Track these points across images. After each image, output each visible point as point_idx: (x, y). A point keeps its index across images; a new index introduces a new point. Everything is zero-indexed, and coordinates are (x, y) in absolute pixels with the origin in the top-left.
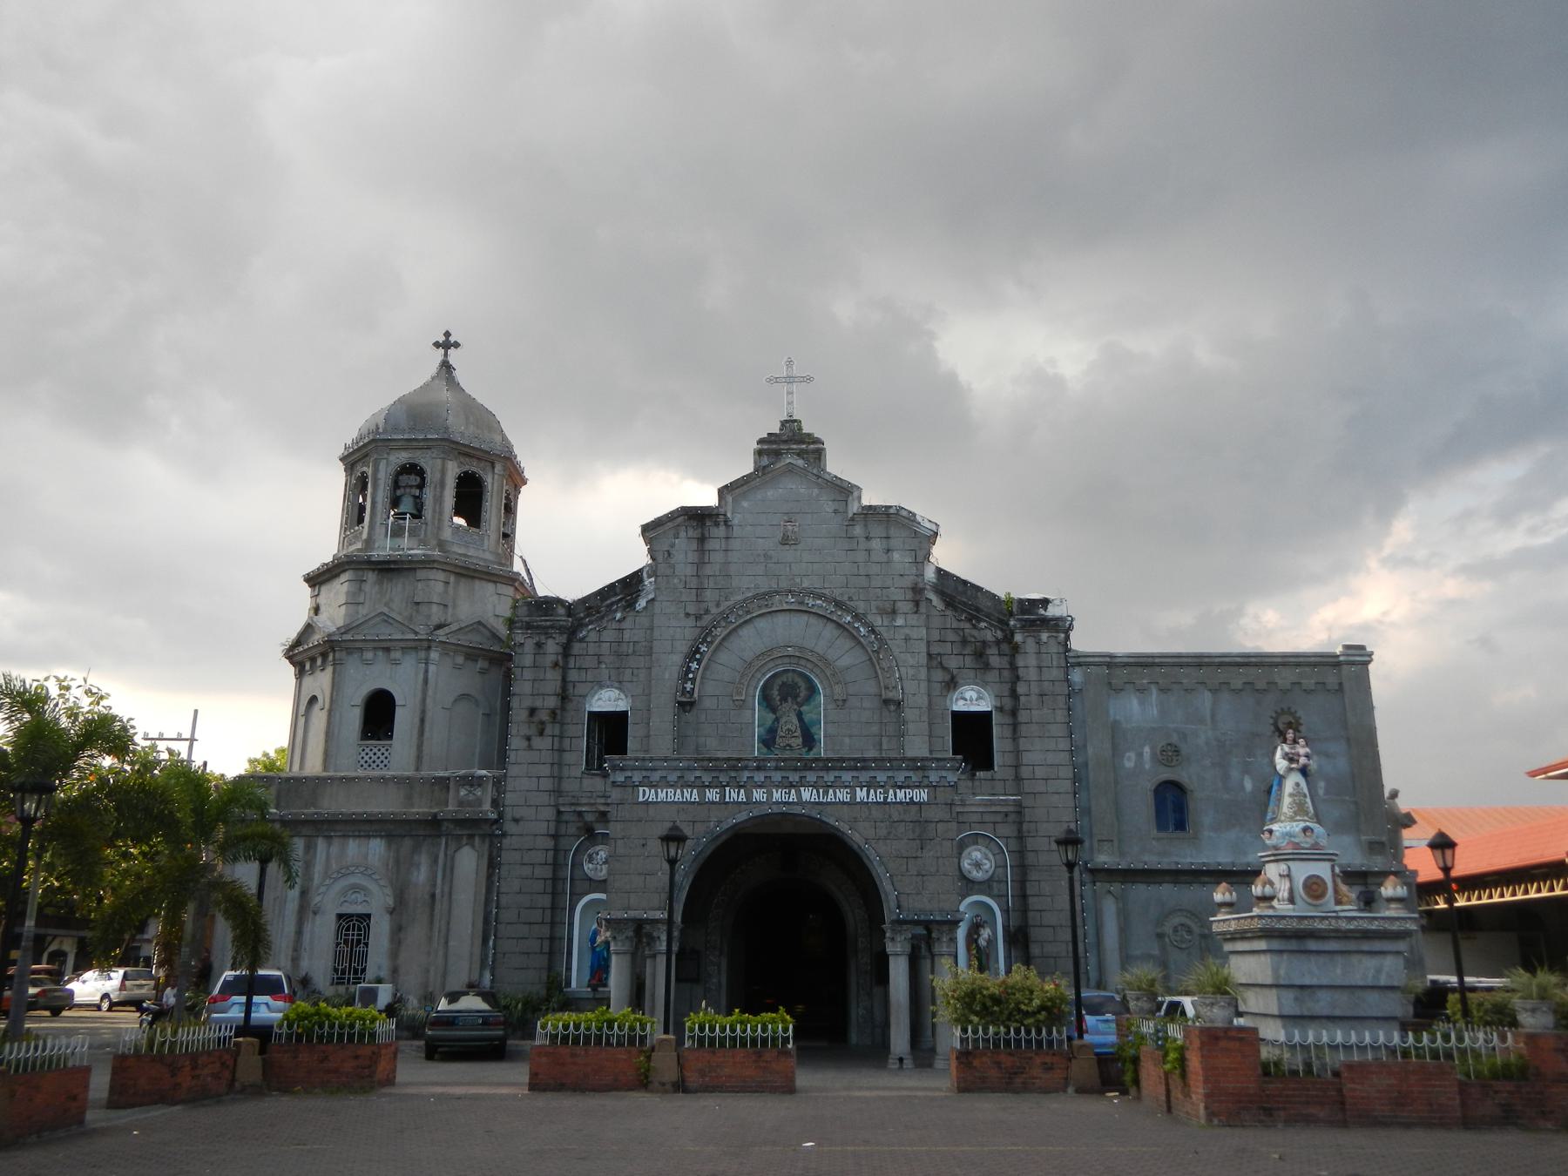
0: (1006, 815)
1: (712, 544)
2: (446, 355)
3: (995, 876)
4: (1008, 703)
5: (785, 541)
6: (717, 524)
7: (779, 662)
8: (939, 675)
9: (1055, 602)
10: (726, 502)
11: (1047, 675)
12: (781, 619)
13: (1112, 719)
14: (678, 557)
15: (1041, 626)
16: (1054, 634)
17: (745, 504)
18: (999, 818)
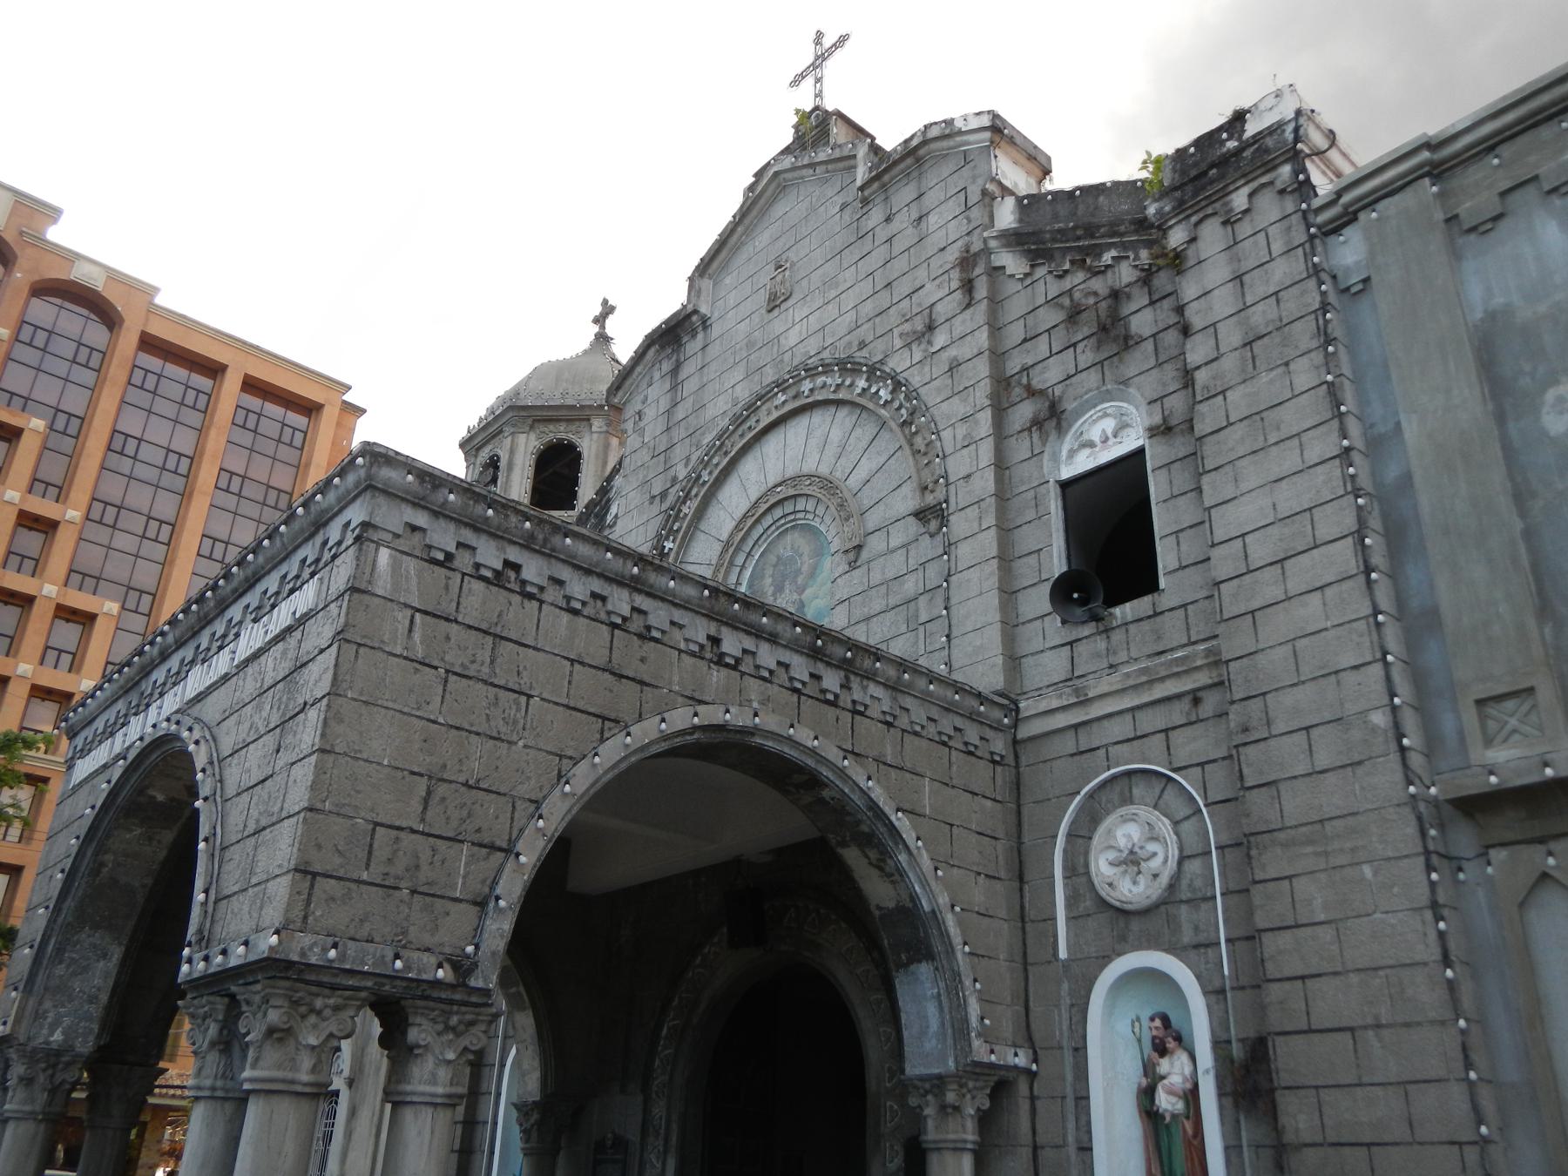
0: (1195, 698)
1: (688, 369)
2: (602, 327)
3: (1184, 882)
4: (1177, 403)
5: (775, 303)
6: (694, 336)
7: (768, 520)
8: (1024, 412)
9: (1262, 107)
10: (699, 292)
11: (1258, 287)
12: (773, 443)
13: (1479, 315)
14: (650, 413)
15: (1222, 177)
16: (1264, 180)
17: (728, 281)
18: (1177, 714)
